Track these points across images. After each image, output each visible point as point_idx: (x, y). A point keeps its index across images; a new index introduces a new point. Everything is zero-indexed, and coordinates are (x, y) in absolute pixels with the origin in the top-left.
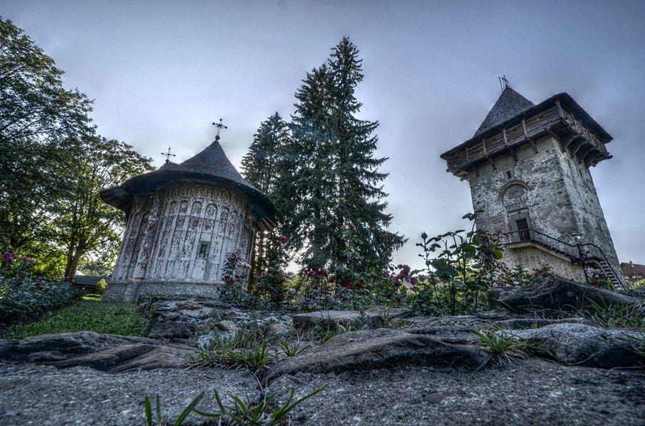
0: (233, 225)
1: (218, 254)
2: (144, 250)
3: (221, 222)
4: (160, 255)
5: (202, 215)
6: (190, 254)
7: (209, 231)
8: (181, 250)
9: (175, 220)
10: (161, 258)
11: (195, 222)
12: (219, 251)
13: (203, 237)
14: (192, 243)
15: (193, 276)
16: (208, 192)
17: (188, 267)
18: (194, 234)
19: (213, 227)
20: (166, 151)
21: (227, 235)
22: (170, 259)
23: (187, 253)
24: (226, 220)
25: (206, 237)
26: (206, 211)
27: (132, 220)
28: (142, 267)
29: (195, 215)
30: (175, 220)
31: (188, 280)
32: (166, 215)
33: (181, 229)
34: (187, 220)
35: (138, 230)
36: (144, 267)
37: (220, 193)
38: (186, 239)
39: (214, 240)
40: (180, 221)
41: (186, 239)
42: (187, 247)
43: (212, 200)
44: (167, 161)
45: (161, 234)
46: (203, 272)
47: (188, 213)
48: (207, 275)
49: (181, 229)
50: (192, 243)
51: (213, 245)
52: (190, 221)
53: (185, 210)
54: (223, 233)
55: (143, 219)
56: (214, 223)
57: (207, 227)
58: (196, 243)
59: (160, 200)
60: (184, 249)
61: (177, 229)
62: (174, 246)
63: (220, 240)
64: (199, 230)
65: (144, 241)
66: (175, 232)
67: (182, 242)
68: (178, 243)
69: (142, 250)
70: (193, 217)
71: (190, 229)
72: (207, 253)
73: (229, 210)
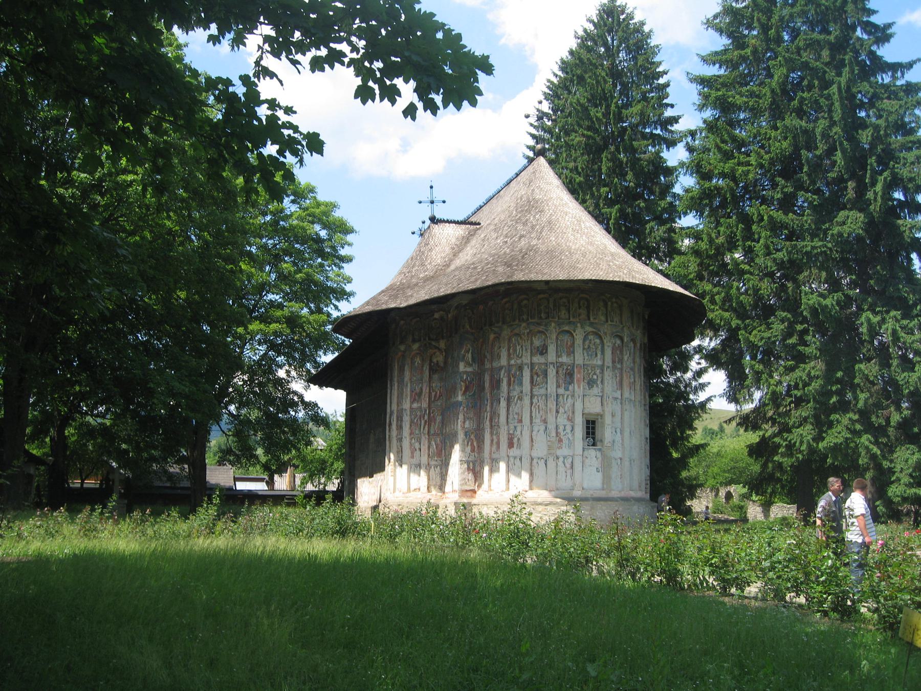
0: (632, 369)
1: (618, 437)
2: (466, 435)
3: (614, 368)
4: (511, 445)
5: (579, 358)
6: (571, 444)
7: (596, 390)
8: (554, 434)
9: (527, 374)
10: (514, 452)
12: (618, 431)
13: (587, 404)
14: (571, 420)
15: (585, 486)
16: (580, 308)
17: (572, 467)
18: (570, 399)
19: (602, 382)
20: (426, 196)
21: (627, 394)
22: (534, 454)
23: (565, 441)
24: (621, 361)
25: (594, 407)
26: (584, 349)
27: (406, 367)
28: (468, 469)
29: (564, 359)
30: (527, 374)
31: (577, 493)
32: (504, 362)
33: (543, 391)
34: (552, 372)
35: (426, 390)
37: (601, 304)
38: (557, 412)
39: (608, 410)
40: (539, 375)
41: (557, 412)
42: (561, 428)
43: (591, 325)
45: (503, 403)
46: (600, 475)
47: (552, 356)
48: (607, 479)
49: (543, 391)
50: (571, 420)
51: (608, 419)
52: (557, 372)
53: (543, 351)
54: (619, 392)
55: (430, 365)
56: (602, 372)
57: (591, 383)
58: (579, 421)
59: (471, 326)
60: (557, 433)
61: (535, 393)
62: (536, 428)
63: (617, 408)
64: (578, 388)
65: (461, 417)
66: (532, 397)
67: (551, 419)
68: (545, 421)
69: (461, 436)
70: (562, 364)
71: (561, 391)
72: (598, 435)
73: (621, 339)
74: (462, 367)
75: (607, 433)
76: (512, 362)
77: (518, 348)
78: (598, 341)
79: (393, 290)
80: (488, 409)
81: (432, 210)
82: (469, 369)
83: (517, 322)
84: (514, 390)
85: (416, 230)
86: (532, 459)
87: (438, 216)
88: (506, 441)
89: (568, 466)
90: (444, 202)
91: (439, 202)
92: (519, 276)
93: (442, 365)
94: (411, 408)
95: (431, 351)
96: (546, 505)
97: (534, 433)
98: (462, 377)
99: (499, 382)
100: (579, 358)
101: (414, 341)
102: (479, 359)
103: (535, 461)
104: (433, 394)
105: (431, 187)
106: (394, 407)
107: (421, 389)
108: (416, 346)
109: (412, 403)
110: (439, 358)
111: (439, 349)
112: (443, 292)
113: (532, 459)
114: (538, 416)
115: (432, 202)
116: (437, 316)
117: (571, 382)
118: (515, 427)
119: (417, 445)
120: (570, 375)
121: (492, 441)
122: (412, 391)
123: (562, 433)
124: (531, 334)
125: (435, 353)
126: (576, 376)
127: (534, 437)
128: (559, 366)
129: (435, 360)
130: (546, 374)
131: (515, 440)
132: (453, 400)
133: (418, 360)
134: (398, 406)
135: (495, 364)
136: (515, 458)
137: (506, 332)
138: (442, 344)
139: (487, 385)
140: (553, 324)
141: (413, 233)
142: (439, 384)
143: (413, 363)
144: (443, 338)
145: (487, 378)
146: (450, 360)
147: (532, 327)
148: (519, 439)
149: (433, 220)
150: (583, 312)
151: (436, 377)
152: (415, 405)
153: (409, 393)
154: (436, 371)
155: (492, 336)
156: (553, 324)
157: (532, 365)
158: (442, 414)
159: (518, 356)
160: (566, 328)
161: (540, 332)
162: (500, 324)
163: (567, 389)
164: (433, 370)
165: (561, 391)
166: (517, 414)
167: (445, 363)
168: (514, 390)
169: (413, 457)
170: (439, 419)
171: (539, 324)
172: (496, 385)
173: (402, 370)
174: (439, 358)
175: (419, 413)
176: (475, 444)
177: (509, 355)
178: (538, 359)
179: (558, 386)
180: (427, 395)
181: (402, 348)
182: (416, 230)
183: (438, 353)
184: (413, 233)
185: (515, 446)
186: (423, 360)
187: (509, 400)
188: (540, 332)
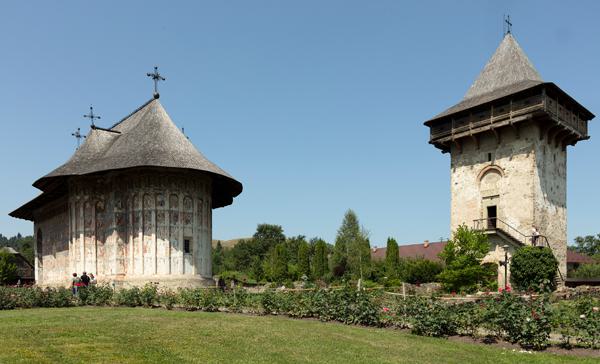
4: (145, 251)
7: (189, 225)
9: (153, 215)
11: (175, 217)
25: (189, 234)
29: (173, 209)
34: (167, 215)
35: (93, 221)
36: (122, 262)
40: (159, 216)
44: (93, 127)
45: (140, 229)
47: (167, 207)
49: (162, 224)
51: (195, 240)
53: (162, 204)
57: (187, 222)
64: (180, 224)
75: (194, 246)
92: (151, 163)
95: (95, 201)
99: (138, 218)
100: (181, 208)
101: (85, 194)
102: (125, 206)
106: (74, 230)
108: (86, 197)
110: (101, 205)
111: (100, 200)
112: (106, 168)
116: (99, 181)
117: (177, 221)
120: (177, 217)
124: (156, 195)
126: (180, 218)
128: (170, 212)
130: (164, 215)
135: (136, 210)
137: (142, 193)
138: (102, 197)
139: (131, 220)
145: (131, 216)
149: (93, 127)
151: (99, 215)
152: (87, 229)
157: (156, 211)
164: (98, 210)
172: (136, 220)
173: (77, 210)
178: (159, 208)
179: (170, 222)
181: (78, 198)
186: (91, 205)
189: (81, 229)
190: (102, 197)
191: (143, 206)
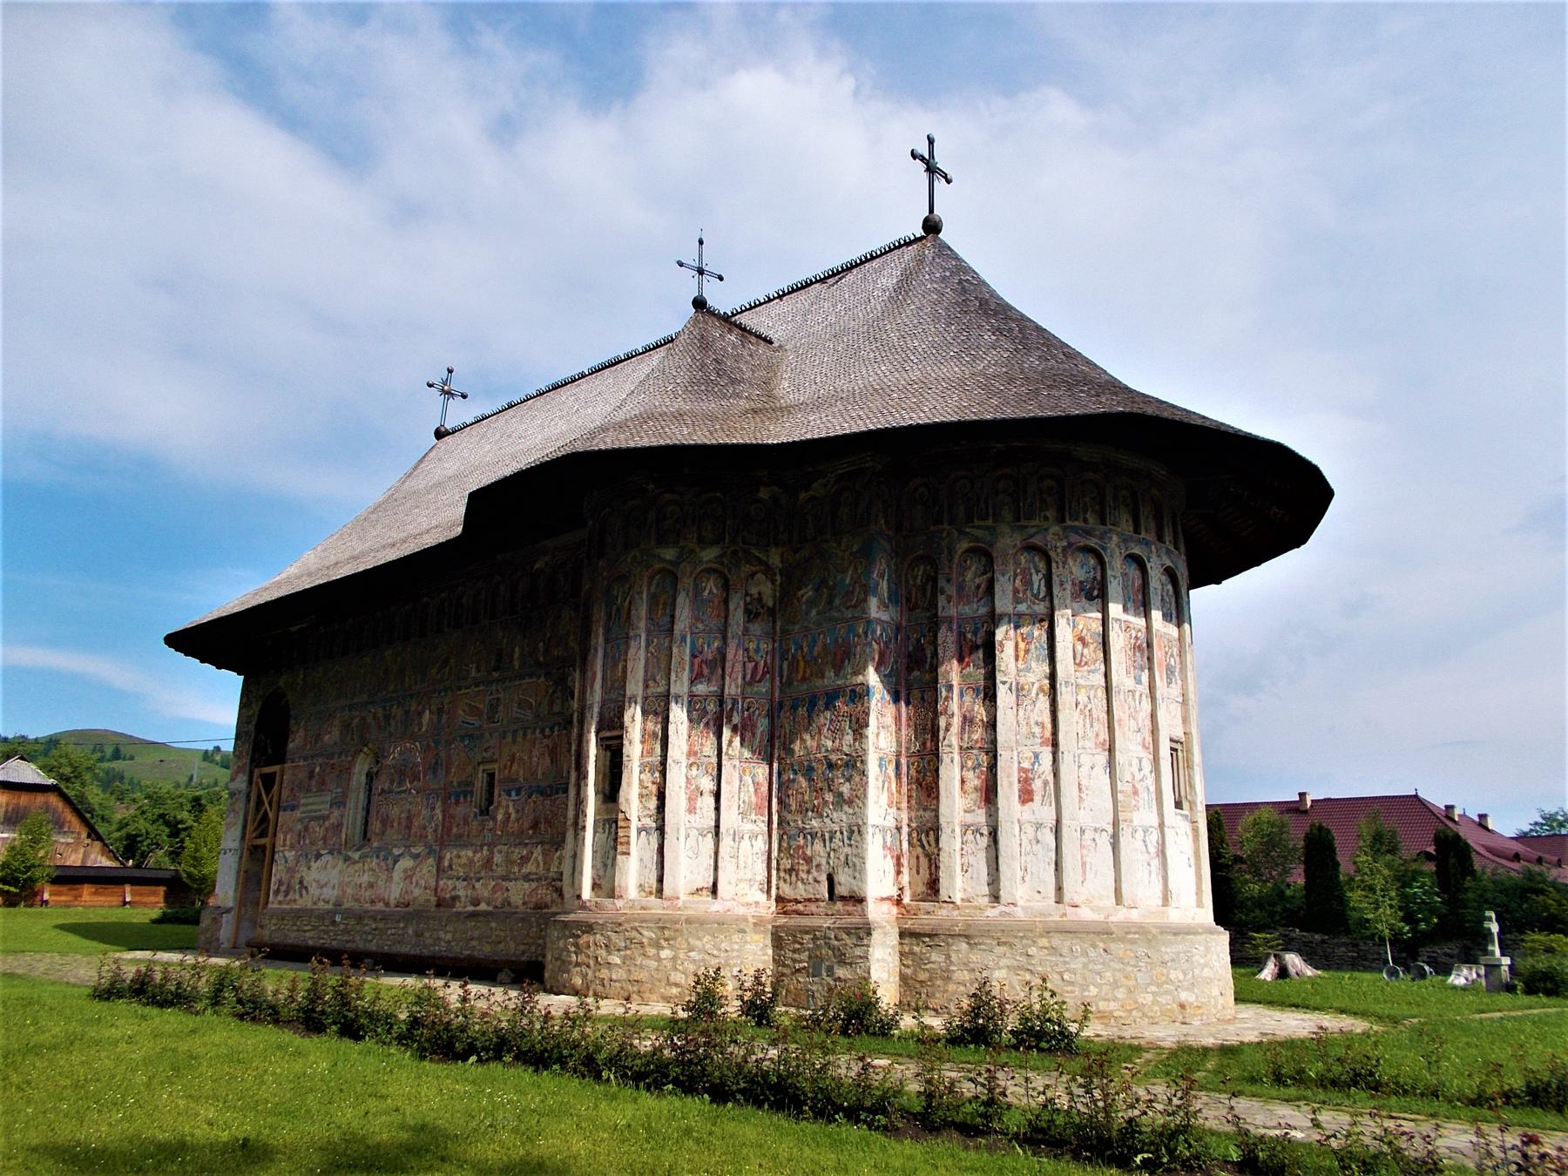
2: (880, 766)
4: (1026, 796)
20: (691, 258)
22: (1085, 818)
23: (1143, 795)
27: (682, 600)
42: (1135, 762)
43: (1168, 552)
59: (887, 523)
74: (874, 609)
76: (1022, 608)
77: (1036, 578)
78: (1170, 587)
79: (592, 435)
80: (954, 706)
81: (700, 288)
82: (885, 617)
83: (1036, 522)
84: (1028, 669)
85: (437, 380)
86: (1083, 831)
87: (711, 302)
88: (1016, 786)
89: (1153, 850)
90: (721, 278)
91: (712, 274)
93: (770, 604)
94: (692, 696)
95: (747, 568)
96: (1133, 942)
97: (1085, 770)
98: (874, 632)
101: (701, 541)
103: (1088, 835)
104: (750, 666)
105: (701, 242)
107: (722, 656)
108: (709, 554)
109: (692, 682)
113: (1083, 831)
114: (1090, 734)
115: (701, 272)
116: (764, 494)
118: (1036, 756)
119: (708, 784)
121: (963, 782)
122: (693, 656)
123: (1138, 777)
125: (753, 575)
127: (1084, 782)
129: (754, 591)
131: (1037, 785)
132: (830, 680)
133: (711, 587)
134: (646, 686)
135: (967, 610)
136: (1039, 826)
137: (1008, 541)
140: (1115, 538)
141: (430, 385)
142: (763, 646)
143: (698, 591)
144: (777, 545)
146: (807, 593)
147: (1074, 538)
148: (1046, 783)
150: (1152, 525)
151: (757, 628)
152: (701, 688)
153: (687, 658)
154: (757, 615)
155: (965, 545)
156: (1115, 538)
158: (772, 716)
159: (1036, 596)
160: (1137, 551)
161: (1088, 550)
162: (990, 522)
163: (1139, 682)
164: (751, 615)
165: (1129, 683)
166: (1041, 725)
167: (786, 596)
168: (1028, 669)
169: (691, 810)
170: (762, 725)
171: (1088, 533)
174: (765, 589)
175: (712, 707)
176: (894, 785)
177: (1016, 591)
180: (739, 667)
181: (669, 554)
182: (437, 380)
183: (760, 576)
184: (430, 385)
185: (1037, 797)
186: (726, 587)
187: (1019, 691)
188: (1088, 550)
189: (680, 686)
190: (775, 559)
191: (1017, 601)
